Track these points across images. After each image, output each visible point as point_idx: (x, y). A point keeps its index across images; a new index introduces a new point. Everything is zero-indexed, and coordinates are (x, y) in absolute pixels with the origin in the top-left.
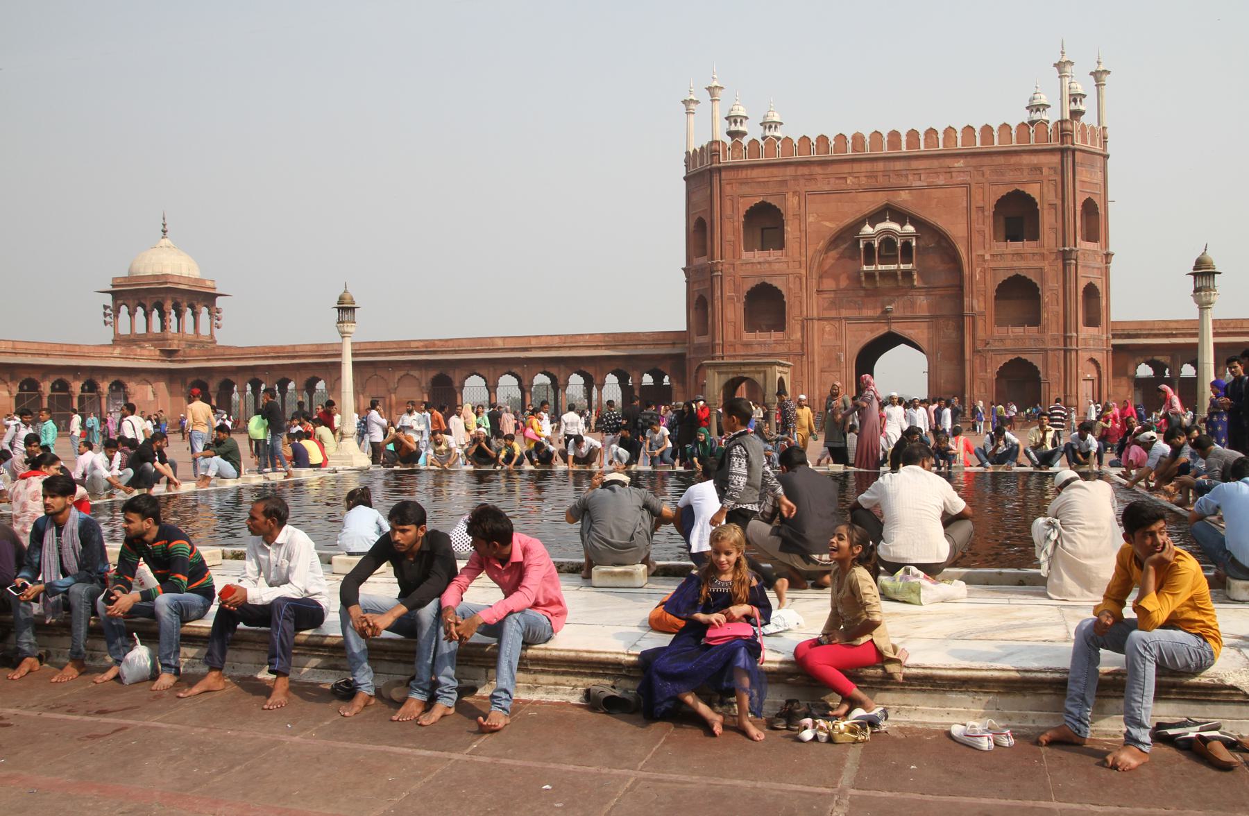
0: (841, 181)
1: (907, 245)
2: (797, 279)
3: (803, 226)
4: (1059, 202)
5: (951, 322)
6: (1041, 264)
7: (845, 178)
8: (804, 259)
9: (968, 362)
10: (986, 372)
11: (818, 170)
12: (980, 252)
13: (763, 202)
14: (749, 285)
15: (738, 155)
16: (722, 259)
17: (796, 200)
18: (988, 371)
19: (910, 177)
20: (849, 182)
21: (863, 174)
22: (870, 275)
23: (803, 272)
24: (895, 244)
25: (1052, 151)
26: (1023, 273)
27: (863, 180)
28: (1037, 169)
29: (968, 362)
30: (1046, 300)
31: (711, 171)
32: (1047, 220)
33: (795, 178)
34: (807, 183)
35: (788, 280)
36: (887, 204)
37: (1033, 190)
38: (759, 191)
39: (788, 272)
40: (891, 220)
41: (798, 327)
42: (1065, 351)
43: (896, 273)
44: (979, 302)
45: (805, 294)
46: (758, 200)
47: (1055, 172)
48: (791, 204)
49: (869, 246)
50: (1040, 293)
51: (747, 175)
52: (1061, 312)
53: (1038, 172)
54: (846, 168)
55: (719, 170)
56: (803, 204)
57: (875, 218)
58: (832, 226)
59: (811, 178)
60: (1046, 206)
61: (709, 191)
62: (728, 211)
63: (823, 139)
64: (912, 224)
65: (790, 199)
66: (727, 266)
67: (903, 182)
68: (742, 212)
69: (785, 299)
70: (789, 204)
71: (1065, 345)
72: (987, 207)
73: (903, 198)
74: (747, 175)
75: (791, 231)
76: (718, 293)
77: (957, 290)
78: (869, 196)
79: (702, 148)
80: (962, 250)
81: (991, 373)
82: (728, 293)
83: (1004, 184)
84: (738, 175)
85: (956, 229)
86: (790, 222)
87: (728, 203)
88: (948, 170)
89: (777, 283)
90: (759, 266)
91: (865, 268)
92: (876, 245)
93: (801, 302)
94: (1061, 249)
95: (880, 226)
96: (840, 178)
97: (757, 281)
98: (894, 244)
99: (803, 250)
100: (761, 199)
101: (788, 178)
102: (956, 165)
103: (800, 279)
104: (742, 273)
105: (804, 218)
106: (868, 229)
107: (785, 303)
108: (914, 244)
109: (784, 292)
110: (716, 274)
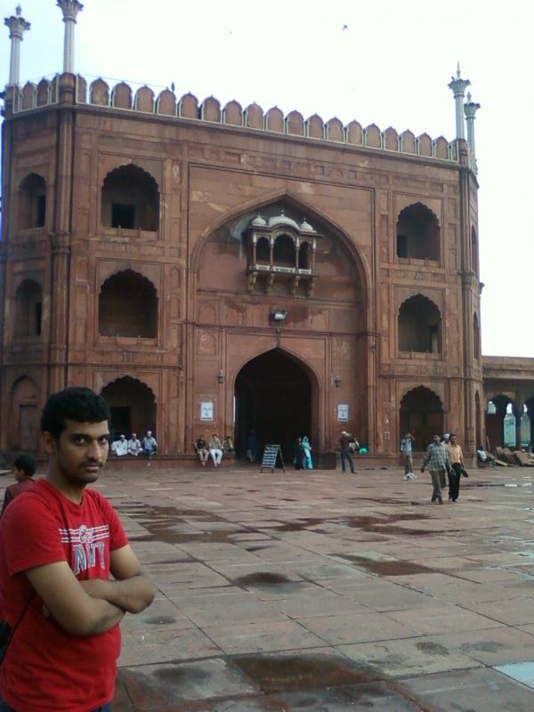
0: (234, 158)
1: (305, 246)
2: (176, 271)
3: (184, 206)
4: (459, 223)
5: (344, 343)
6: (442, 285)
7: (239, 156)
8: (185, 246)
9: (372, 389)
10: (390, 401)
11: (206, 139)
12: (386, 266)
13: (131, 166)
14: (106, 272)
15: (102, 100)
16: (70, 231)
17: (176, 170)
18: (393, 399)
19: (312, 169)
20: (242, 160)
21: (262, 155)
22: (263, 278)
23: (183, 262)
24: (292, 243)
25: (451, 168)
26: (425, 293)
27: (259, 162)
28: (438, 184)
29: (372, 389)
30: (447, 325)
31: (59, 113)
32: (447, 239)
33: (176, 143)
34: (191, 152)
35: (162, 271)
36: (286, 195)
37: (435, 206)
38: (129, 151)
39: (163, 260)
40: (287, 215)
41: (174, 332)
42: (466, 380)
43: (295, 277)
44: (387, 322)
45: (185, 291)
46: (126, 162)
47: (454, 191)
48: (169, 175)
49: (263, 242)
50: (441, 316)
51: (111, 126)
52: (461, 339)
53: (440, 188)
54: (239, 142)
55: (74, 112)
56: (185, 175)
57: (268, 209)
58: (220, 209)
59: (198, 147)
60: (446, 225)
61: (54, 141)
62: (83, 166)
63: (211, 102)
64: (310, 222)
65: (169, 168)
66: (77, 242)
67: (303, 172)
68: (103, 175)
69: (158, 295)
70: (167, 174)
71: (465, 375)
72: (391, 217)
73: (305, 189)
74: (111, 126)
75: (168, 208)
76: (61, 280)
77: (359, 305)
78: (266, 183)
79: (44, 82)
80: (365, 257)
81: (395, 403)
82: (79, 278)
83: (408, 195)
84: (100, 124)
85: (360, 236)
86: (167, 198)
87: (84, 159)
88: (352, 169)
89: (150, 273)
90: (123, 248)
91: (258, 267)
92: (272, 242)
93: (179, 301)
94: (461, 272)
95: (275, 221)
96: (233, 154)
97: (123, 267)
98: (291, 243)
99: (184, 235)
100: (130, 161)
101: (167, 141)
102: (361, 165)
103: (179, 272)
104: (99, 255)
105: (185, 195)
106: (260, 221)
107: (157, 299)
108: (314, 246)
109: (157, 286)
110: (61, 251)
